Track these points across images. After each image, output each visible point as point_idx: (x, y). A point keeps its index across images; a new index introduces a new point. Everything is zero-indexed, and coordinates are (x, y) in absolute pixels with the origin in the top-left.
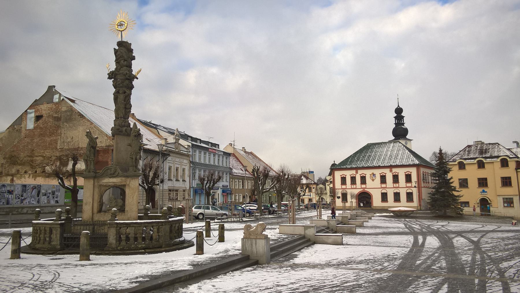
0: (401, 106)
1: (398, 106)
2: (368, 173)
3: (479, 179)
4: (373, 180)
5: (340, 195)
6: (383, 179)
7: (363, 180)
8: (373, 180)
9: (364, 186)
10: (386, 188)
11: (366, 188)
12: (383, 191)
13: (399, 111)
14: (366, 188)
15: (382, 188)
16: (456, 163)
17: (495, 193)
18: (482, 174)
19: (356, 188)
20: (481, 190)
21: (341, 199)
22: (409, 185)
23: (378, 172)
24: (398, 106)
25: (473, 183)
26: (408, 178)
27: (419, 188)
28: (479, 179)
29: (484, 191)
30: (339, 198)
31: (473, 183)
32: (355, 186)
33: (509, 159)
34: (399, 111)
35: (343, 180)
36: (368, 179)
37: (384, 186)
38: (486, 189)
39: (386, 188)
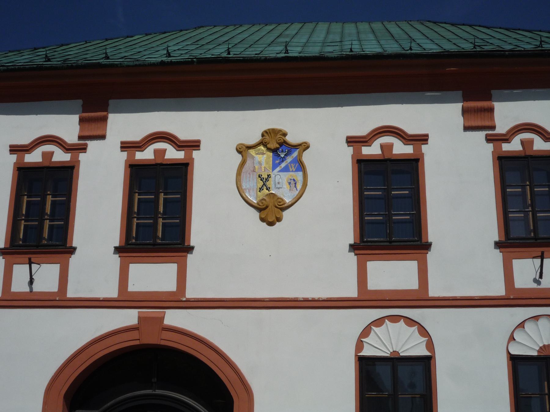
2: (217, 137)
4: (270, 211)
6: (390, 206)
7: (159, 208)
8: (270, 211)
9: (153, 276)
10: (420, 299)
11: (177, 300)
12: (379, 345)
14: (177, 300)
15: (366, 299)
19: (58, 301)
23: (331, 132)
32: (46, 277)
36: (215, 206)
37: (392, 274)
39: (420, 299)
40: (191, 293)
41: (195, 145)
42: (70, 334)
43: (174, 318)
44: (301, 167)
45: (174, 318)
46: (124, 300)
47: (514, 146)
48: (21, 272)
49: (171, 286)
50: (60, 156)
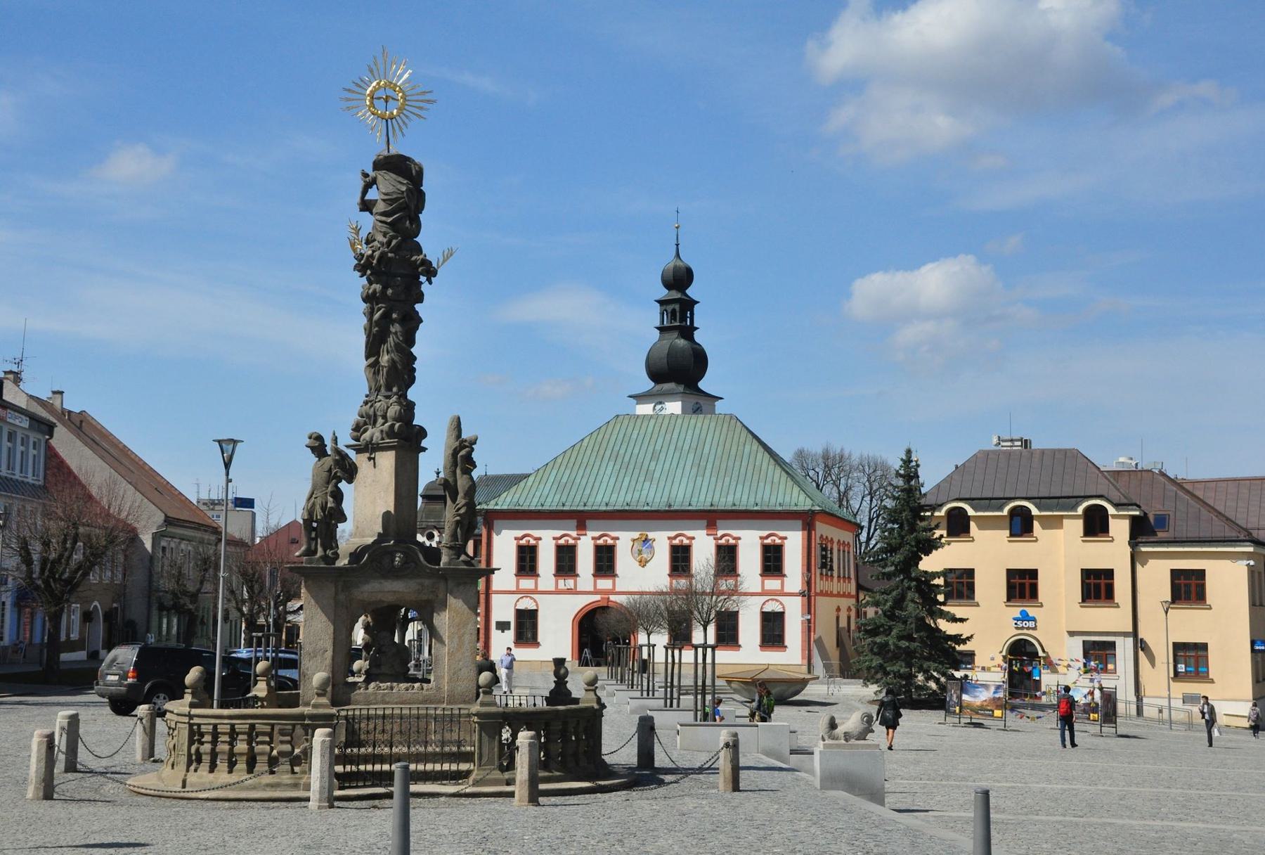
0: (688, 259)
1: (678, 255)
3: (1011, 573)
4: (643, 563)
5: (510, 617)
7: (605, 561)
8: (643, 563)
9: (605, 584)
13: (679, 279)
16: (942, 513)
17: (1060, 621)
18: (1022, 555)
20: (1016, 612)
21: (510, 634)
22: (773, 584)
24: (678, 255)
25: (991, 586)
26: (772, 561)
27: (808, 594)
28: (1011, 573)
29: (1025, 617)
30: (503, 626)
31: (991, 586)
32: (570, 583)
33: (1111, 510)
34: (679, 279)
35: (527, 560)
36: (624, 559)
38: (1032, 612)
40: (617, 589)
41: (617, 538)
42: (580, 603)
43: (613, 598)
44: (651, 547)
45: (613, 598)
46: (596, 592)
47: (723, 541)
48: (561, 582)
49: (610, 587)
50: (571, 542)
